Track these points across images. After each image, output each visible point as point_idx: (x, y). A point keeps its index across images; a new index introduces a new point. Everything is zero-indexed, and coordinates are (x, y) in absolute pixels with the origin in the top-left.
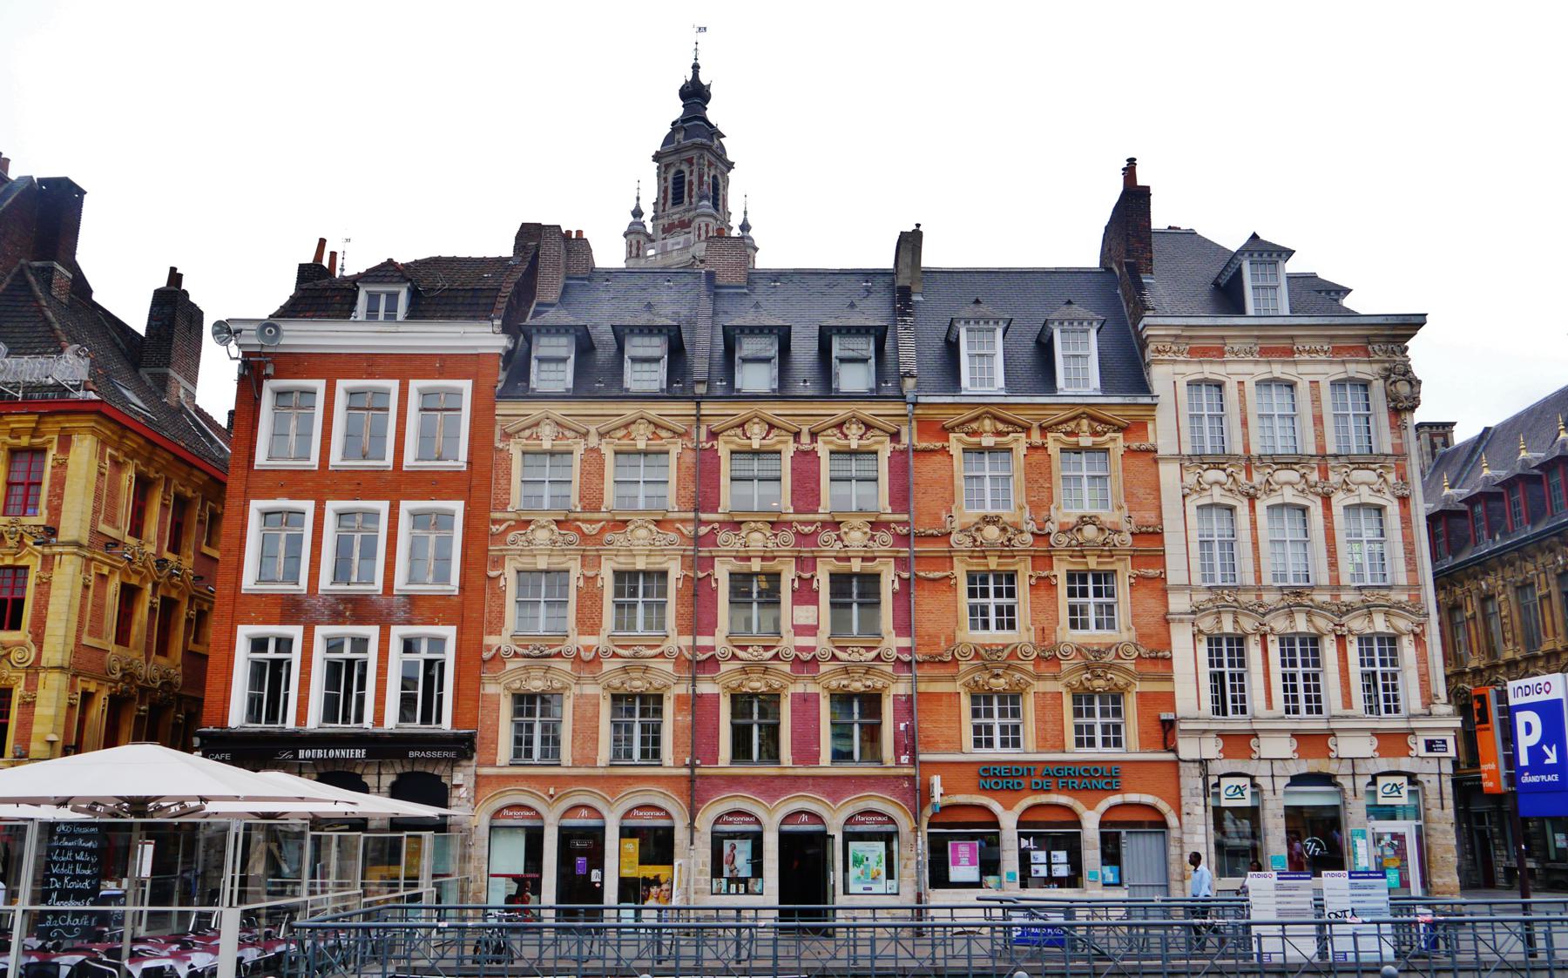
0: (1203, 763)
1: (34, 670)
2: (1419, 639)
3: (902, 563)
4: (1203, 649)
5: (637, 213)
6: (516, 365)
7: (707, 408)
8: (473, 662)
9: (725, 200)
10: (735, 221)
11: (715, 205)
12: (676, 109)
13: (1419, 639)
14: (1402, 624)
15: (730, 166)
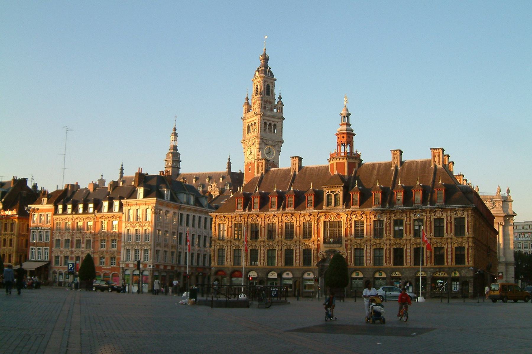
0: (123, 268)
1: (13, 252)
2: (151, 249)
3: (94, 238)
4: (125, 251)
5: (247, 99)
6: (56, 209)
7: (74, 216)
8: (51, 252)
9: (273, 91)
10: (277, 98)
11: (268, 94)
12: (259, 63)
13: (151, 249)
14: (149, 247)
15: (275, 80)
